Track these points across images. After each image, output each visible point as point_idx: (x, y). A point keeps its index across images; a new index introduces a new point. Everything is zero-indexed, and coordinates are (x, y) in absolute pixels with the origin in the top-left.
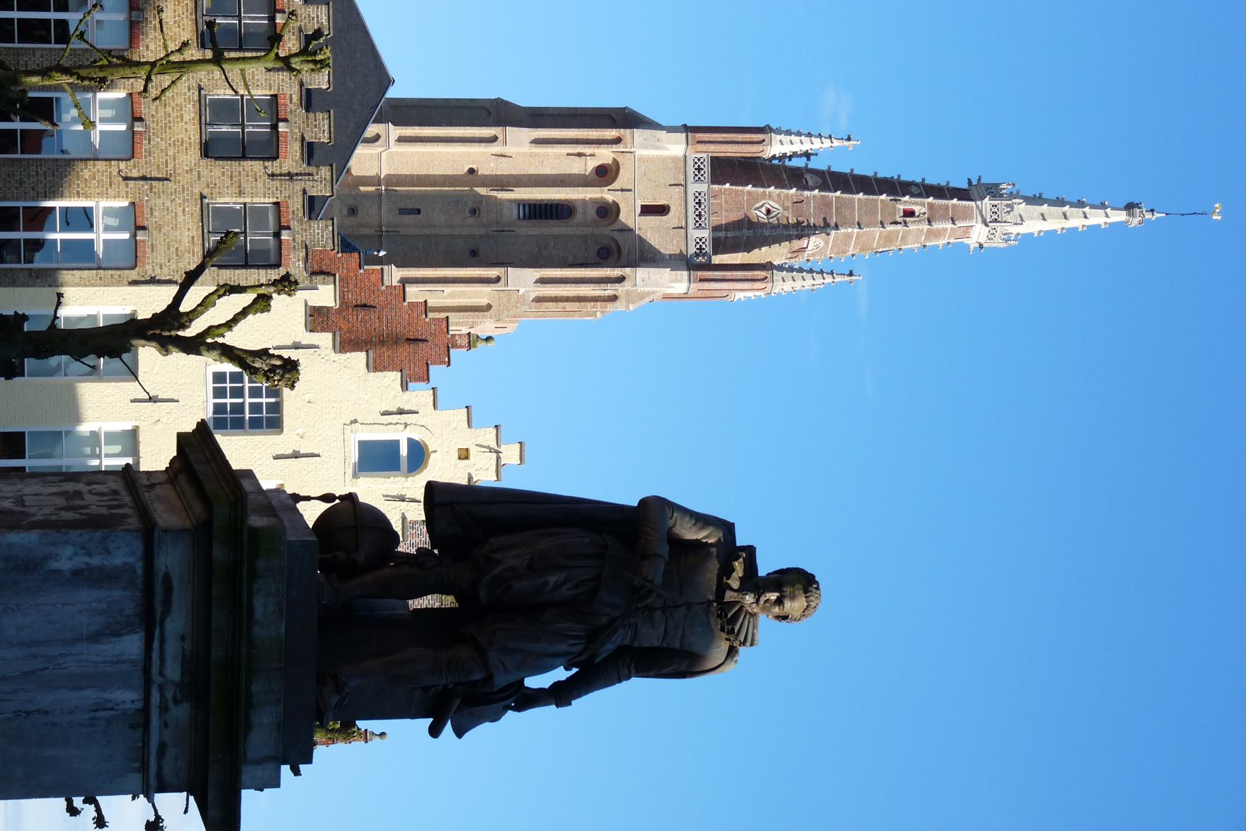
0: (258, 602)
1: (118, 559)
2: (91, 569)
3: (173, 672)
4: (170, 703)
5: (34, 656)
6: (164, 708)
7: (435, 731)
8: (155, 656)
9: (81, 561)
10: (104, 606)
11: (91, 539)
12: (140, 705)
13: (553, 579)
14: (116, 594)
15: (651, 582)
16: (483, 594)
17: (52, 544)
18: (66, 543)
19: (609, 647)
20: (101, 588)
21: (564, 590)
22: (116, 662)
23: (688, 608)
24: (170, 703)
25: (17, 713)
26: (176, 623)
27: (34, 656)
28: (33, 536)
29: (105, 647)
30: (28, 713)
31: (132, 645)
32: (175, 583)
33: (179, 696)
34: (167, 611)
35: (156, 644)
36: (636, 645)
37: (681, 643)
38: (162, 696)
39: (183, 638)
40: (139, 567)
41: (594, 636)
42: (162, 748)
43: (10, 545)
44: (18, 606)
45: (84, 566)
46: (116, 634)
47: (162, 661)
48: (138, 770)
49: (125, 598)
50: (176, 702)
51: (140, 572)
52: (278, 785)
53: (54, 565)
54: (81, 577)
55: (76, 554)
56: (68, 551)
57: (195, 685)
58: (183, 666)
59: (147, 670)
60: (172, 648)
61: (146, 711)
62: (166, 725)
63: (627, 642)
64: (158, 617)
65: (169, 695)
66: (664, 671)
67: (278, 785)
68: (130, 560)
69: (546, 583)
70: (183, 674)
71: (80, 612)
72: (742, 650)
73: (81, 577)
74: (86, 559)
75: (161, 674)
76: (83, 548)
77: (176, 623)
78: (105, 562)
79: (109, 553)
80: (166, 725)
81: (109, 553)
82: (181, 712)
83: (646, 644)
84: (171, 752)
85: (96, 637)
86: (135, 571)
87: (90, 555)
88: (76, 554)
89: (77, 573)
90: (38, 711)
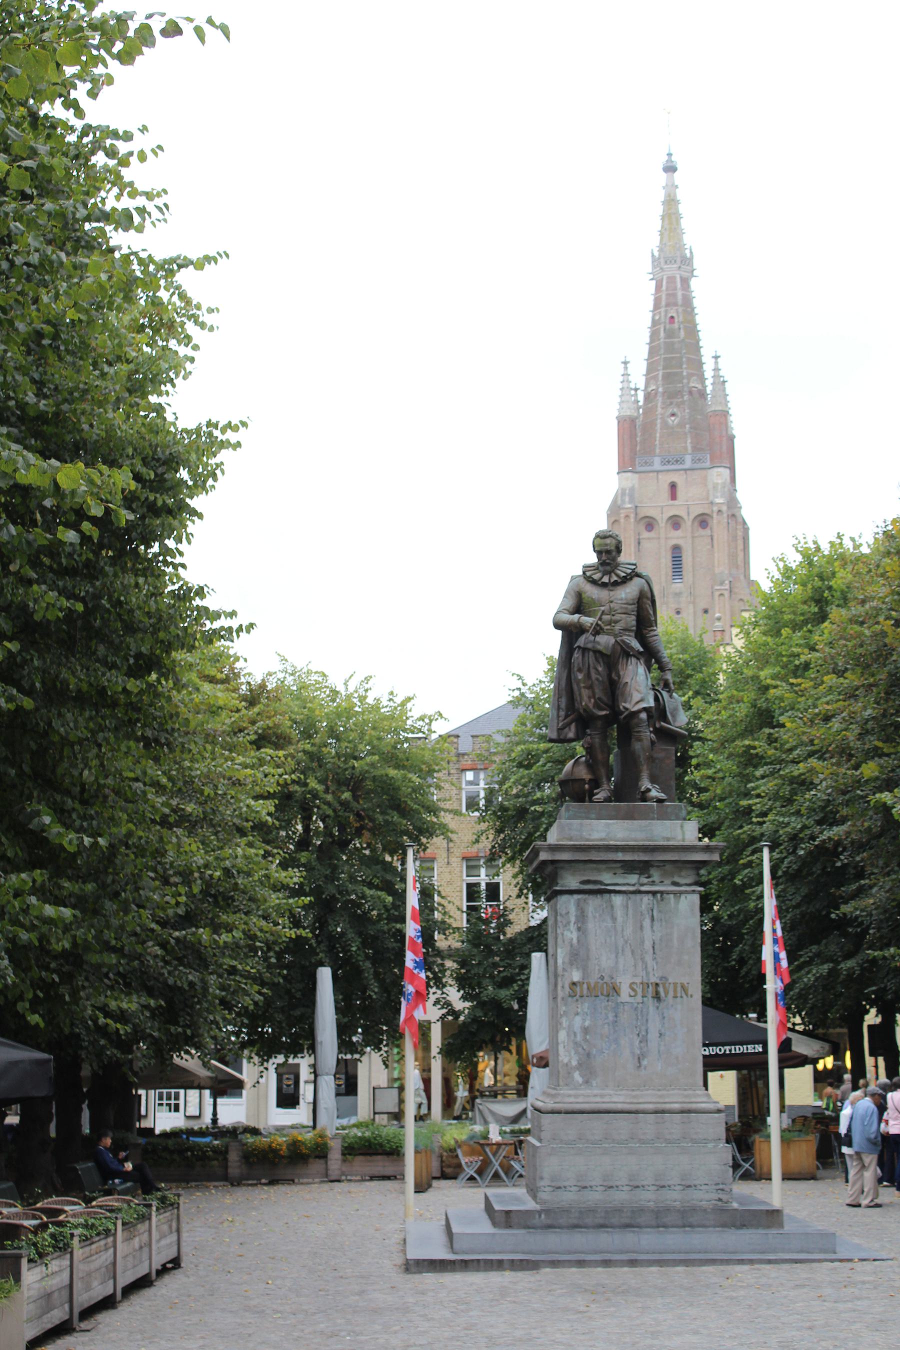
1: (573, 909)
3: (633, 878)
9: (572, 927)
13: (594, 675)
16: (604, 713)
19: (636, 645)
21: (600, 669)
25: (654, 959)
26: (607, 878)
28: (559, 951)
31: (618, 900)
32: (585, 878)
34: (601, 883)
35: (617, 888)
40: (576, 897)
41: (626, 653)
46: (612, 907)
49: (593, 904)
51: (580, 896)
53: (575, 941)
57: (643, 868)
61: (654, 893)
63: (633, 634)
65: (645, 881)
68: (572, 901)
77: (607, 878)
82: (656, 875)
83: (634, 623)
84: (677, 879)
85: (614, 919)
87: (569, 923)
89: (579, 929)
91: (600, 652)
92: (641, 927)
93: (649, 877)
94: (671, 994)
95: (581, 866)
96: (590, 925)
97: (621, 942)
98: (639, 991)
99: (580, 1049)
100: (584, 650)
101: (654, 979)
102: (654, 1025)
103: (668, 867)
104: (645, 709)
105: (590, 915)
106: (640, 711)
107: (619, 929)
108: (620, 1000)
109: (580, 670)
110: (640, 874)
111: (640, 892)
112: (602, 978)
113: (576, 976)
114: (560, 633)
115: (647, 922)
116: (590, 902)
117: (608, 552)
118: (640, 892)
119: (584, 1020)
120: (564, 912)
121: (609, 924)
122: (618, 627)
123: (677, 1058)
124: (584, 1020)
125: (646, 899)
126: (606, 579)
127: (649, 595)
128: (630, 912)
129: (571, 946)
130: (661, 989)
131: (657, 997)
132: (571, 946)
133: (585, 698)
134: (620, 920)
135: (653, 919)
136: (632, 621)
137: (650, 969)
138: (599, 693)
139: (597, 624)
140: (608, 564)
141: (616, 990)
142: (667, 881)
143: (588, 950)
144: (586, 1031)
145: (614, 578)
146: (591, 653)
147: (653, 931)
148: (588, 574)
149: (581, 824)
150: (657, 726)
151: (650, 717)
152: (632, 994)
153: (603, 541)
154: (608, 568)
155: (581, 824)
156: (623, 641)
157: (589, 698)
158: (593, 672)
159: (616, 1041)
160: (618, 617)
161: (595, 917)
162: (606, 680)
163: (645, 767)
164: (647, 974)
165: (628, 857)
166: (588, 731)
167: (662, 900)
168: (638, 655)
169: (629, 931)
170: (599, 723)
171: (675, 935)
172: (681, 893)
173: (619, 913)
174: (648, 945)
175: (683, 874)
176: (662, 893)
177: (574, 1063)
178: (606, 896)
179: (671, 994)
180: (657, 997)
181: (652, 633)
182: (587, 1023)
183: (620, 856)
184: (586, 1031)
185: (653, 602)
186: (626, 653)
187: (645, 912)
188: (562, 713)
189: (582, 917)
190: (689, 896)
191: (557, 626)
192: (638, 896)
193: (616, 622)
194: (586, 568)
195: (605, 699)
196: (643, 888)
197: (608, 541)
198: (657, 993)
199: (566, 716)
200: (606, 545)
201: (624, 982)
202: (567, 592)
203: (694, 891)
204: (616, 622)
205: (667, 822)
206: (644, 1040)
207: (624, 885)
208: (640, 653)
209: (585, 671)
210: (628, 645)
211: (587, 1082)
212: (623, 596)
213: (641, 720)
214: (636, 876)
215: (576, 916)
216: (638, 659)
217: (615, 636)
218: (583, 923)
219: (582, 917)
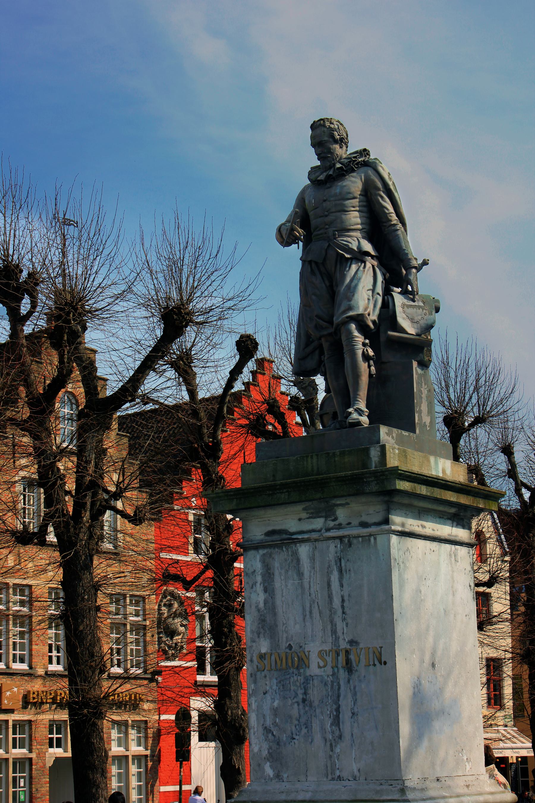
2: (264, 581)
3: (318, 523)
4: (337, 523)
5: (311, 612)
6: (339, 527)
8: (306, 536)
9: (259, 588)
10: (283, 571)
12: (338, 541)
14: (277, 565)
17: (251, 606)
20: (273, 574)
23: (325, 201)
25: (344, 619)
27: (311, 612)
30: (344, 613)
31: (304, 550)
32: (270, 528)
33: (333, 518)
34: (285, 532)
35: (300, 537)
38: (332, 528)
40: (261, 552)
43: (252, 632)
44: (284, 624)
45: (262, 585)
46: (298, 560)
47: (313, 531)
48: (375, 539)
49: (279, 558)
50: (335, 519)
51: (265, 551)
53: (262, 605)
54: (269, 589)
56: (253, 596)
58: (315, 518)
60: (306, 526)
61: (341, 538)
65: (331, 524)
68: (258, 557)
71: (286, 586)
73: (269, 589)
74: (258, 585)
75: (320, 531)
76: (252, 588)
78: (259, 573)
79: (255, 571)
80: (349, 524)
81: (255, 571)
85: (300, 575)
87: (256, 582)
88: (255, 591)
89: (266, 590)
90: (343, 607)
94: (363, 662)
96: (278, 583)
98: (329, 659)
99: (270, 735)
101: (343, 645)
102: (346, 704)
104: (353, 319)
107: (306, 586)
108: (308, 673)
110: (326, 517)
112: (290, 647)
113: (264, 647)
115: (335, 577)
116: (276, 557)
119: (273, 700)
123: (372, 743)
124: (273, 700)
127: (379, 185)
128: (317, 564)
130: (352, 657)
131: (349, 667)
132: (259, 610)
135: (340, 571)
136: (354, 218)
137: (340, 633)
141: (302, 662)
143: (275, 614)
144: (275, 712)
145: (331, 173)
147: (342, 586)
148: (313, 177)
152: (322, 664)
159: (308, 726)
161: (280, 574)
164: (337, 639)
174: (337, 602)
177: (265, 753)
179: (363, 662)
180: (349, 667)
182: (276, 704)
184: (275, 712)
187: (333, 563)
189: (268, 575)
194: (314, 169)
197: (318, 131)
198: (348, 661)
199: (307, 345)
201: (314, 648)
204: (331, 223)
206: (337, 721)
211: (278, 776)
215: (263, 576)
219: (268, 575)
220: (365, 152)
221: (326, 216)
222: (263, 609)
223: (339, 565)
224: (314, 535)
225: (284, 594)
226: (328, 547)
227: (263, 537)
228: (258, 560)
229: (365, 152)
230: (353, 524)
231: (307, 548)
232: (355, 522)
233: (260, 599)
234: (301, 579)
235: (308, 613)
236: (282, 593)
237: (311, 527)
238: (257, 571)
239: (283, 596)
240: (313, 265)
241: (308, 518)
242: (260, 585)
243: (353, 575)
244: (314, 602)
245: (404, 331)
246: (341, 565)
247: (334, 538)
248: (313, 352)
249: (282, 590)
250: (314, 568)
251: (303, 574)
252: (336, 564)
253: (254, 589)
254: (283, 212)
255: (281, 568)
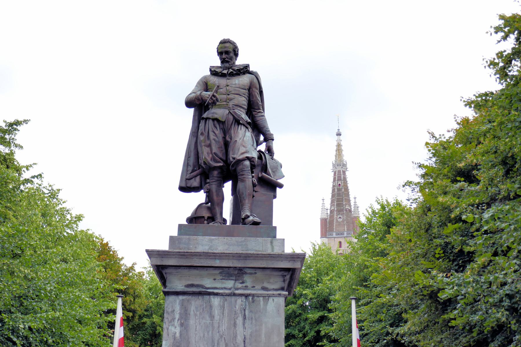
0: (200, 249)
1: (178, 308)
3: (230, 284)
6: (246, 288)
7: (281, 186)
9: (176, 323)
10: (198, 313)
11: (167, 318)
12: (244, 297)
13: (212, 136)
15: (209, 95)
18: (168, 329)
19: (244, 117)
21: (217, 132)
22: (224, 308)
23: (228, 86)
24: (244, 285)
29: (216, 312)
31: (216, 301)
32: (190, 282)
33: (241, 281)
34: (202, 286)
35: (216, 291)
36: (246, 107)
37: (245, 89)
39: (215, 279)
40: (181, 297)
41: (237, 122)
42: (264, 289)
46: (211, 307)
47: (225, 288)
49: (195, 303)
52: (284, 240)
53: (178, 335)
55: (173, 325)
56: (172, 329)
59: (229, 295)
61: (247, 296)
62: (254, 287)
64: (204, 290)
65: (240, 286)
66: (259, 99)
67: (284, 240)
68: (178, 301)
69: (214, 139)
70: (232, 280)
72: (251, 69)
75: (230, 289)
77: (208, 283)
78: (178, 312)
80: (254, 287)
81: (174, 310)
82: (248, 280)
84: (266, 285)
85: (212, 317)
86: (183, 300)
87: (174, 319)
88: (173, 325)
89: (182, 325)
91: (217, 120)
92: (235, 324)
93: (243, 283)
95: (186, 271)
96: (192, 322)
97: (217, 337)
100: (206, 119)
103: (259, 274)
104: (248, 158)
105: (192, 313)
106: (243, 160)
107: (216, 325)
109: (202, 134)
111: (234, 295)
114: (192, 110)
117: (227, 53)
118: (234, 295)
120: (170, 310)
121: (208, 321)
122: (231, 104)
125: (240, 301)
126: (225, 72)
127: (258, 86)
128: (226, 312)
129: (175, 339)
132: (175, 339)
133: (205, 153)
134: (217, 317)
136: (243, 101)
138: (215, 149)
139: (213, 96)
140: (228, 62)
142: (258, 287)
146: (211, 121)
147: (245, 328)
149: (189, 239)
150: (260, 176)
151: (253, 167)
153: (223, 45)
154: (227, 65)
155: (189, 239)
156: (235, 112)
157: (208, 153)
158: (211, 134)
160: (231, 96)
161: (195, 315)
162: (221, 139)
163: (247, 201)
165: (224, 264)
166: (208, 181)
167: (253, 301)
168: (246, 125)
169: (224, 327)
170: (215, 173)
171: (263, 331)
172: (269, 296)
173: (216, 312)
175: (271, 281)
176: (253, 296)
178: (207, 297)
181: (260, 114)
183: (217, 263)
185: (261, 92)
186: (237, 122)
187: (239, 312)
188: (190, 169)
189: (185, 315)
190: (276, 299)
191: (189, 104)
192: (233, 299)
193: (231, 100)
195: (220, 155)
196: (237, 292)
197: (227, 45)
199: (193, 171)
200: (225, 47)
202: (198, 83)
203: (280, 294)
204: (231, 100)
205: (260, 239)
207: (222, 289)
208: (249, 123)
209: (206, 134)
210: (239, 116)
212: (237, 82)
213: (245, 165)
214: (233, 282)
215: (180, 314)
216: (247, 128)
217: (229, 109)
218: (186, 320)
219: (185, 315)
220: (247, 67)
221: (228, 95)
222: (179, 338)
223: (243, 313)
224: (227, 292)
225: (197, 329)
226: (236, 301)
227: (183, 287)
228: (178, 303)
229: (247, 67)
230: (256, 287)
231: (219, 299)
232: (258, 287)
233: (177, 331)
234: (212, 320)
235: (216, 344)
236: (196, 328)
237: (223, 286)
238: (176, 311)
239: (196, 330)
240: (215, 122)
241: (221, 279)
242: (178, 320)
243: (254, 321)
244: (221, 337)
245: (269, 175)
246: (245, 313)
247: (241, 295)
248: (196, 176)
249: (196, 326)
250: (223, 314)
251: (214, 317)
252: (241, 313)
253: (173, 323)
254: (189, 86)
255: (197, 311)
